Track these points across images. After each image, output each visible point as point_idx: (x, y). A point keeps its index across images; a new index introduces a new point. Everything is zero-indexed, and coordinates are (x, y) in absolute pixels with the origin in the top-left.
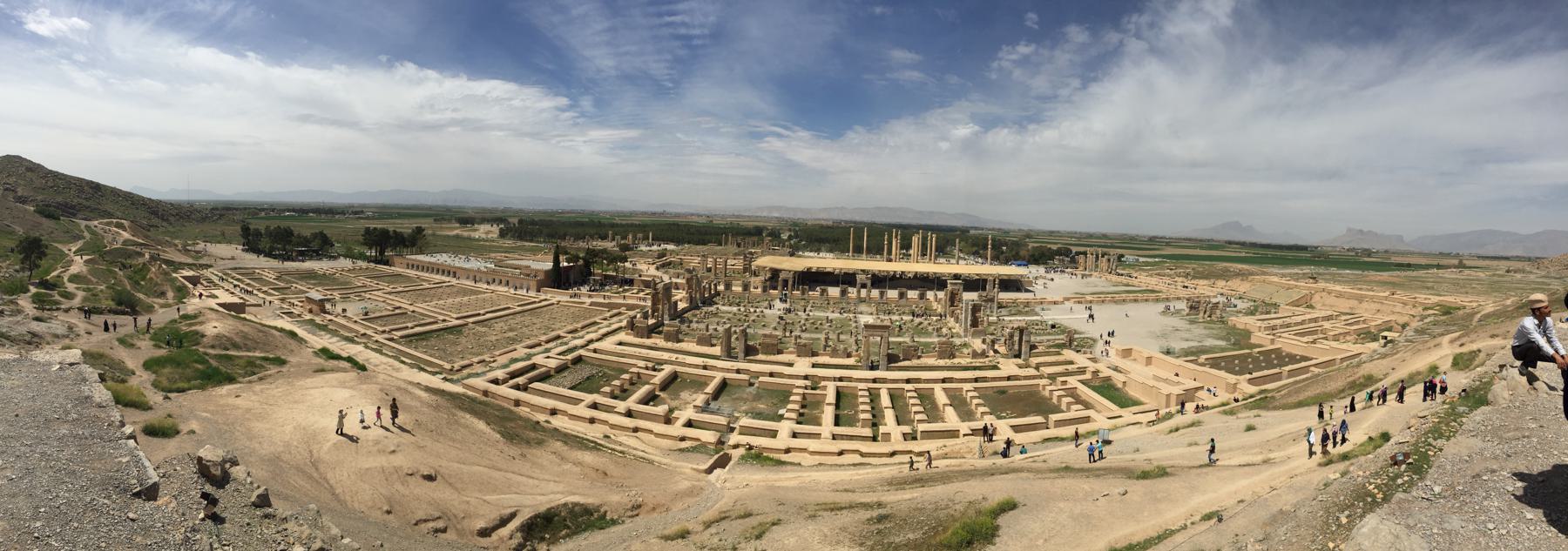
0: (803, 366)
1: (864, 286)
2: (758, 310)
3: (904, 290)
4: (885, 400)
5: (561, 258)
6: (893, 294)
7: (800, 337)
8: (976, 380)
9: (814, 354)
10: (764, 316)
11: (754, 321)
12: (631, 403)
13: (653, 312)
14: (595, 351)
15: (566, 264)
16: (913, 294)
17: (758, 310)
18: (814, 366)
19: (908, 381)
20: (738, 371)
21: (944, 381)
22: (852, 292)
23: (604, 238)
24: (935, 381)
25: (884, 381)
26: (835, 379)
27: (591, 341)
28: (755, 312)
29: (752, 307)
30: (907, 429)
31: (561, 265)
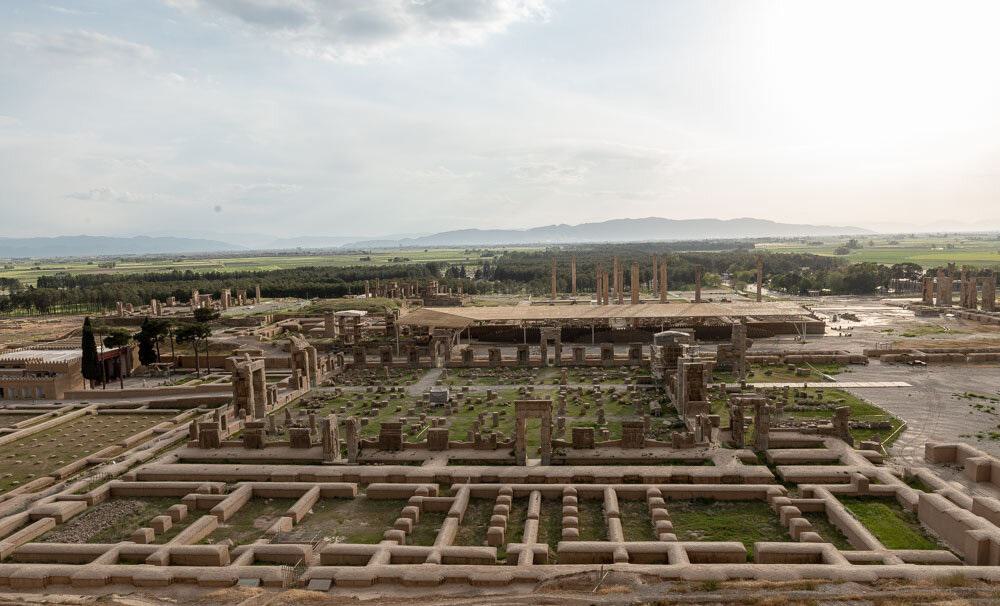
0: (436, 466)
1: (551, 342)
2: (396, 388)
3: (609, 345)
4: (535, 506)
5: (97, 338)
6: (593, 352)
7: (441, 423)
8: (673, 479)
9: (452, 447)
10: (402, 396)
11: (385, 404)
12: (175, 544)
13: (239, 406)
14: (139, 478)
15: (106, 350)
16: (622, 353)
17: (396, 388)
18: (452, 462)
19: (575, 480)
20: (344, 478)
21: (626, 479)
22: (534, 353)
23: (184, 298)
24: (609, 480)
25: (544, 479)
26: (473, 480)
27: (138, 463)
28: (393, 390)
29: (388, 384)
30: (544, 547)
31: (99, 351)
